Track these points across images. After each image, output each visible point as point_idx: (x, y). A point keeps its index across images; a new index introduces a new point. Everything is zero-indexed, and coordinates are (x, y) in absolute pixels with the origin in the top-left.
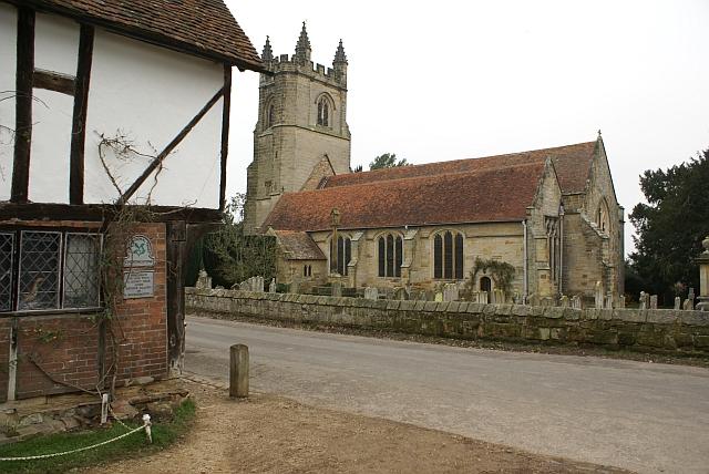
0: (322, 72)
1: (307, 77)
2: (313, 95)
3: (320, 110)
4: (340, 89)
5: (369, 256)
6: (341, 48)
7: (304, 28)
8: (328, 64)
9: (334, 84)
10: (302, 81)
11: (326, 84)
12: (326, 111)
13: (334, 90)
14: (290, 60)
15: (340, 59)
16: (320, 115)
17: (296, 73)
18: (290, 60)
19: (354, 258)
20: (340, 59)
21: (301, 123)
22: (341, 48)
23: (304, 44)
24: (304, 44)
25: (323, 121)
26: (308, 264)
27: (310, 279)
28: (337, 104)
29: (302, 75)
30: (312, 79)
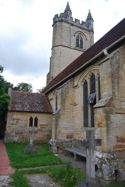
0: (78, 23)
1: (68, 23)
2: (73, 33)
3: (78, 40)
4: (89, 31)
5: (75, 105)
6: (90, 15)
7: (68, 4)
8: (83, 18)
9: (86, 28)
10: (64, 24)
11: (81, 28)
12: (82, 41)
13: (86, 31)
14: (59, 16)
15: (90, 18)
16: (77, 43)
17: (62, 21)
18: (59, 16)
19: (59, 107)
20: (90, 18)
21: (64, 44)
22: (90, 15)
23: (68, 10)
24: (68, 10)
25: (77, 45)
26: (34, 116)
27: (36, 129)
28: (88, 38)
29: (66, 22)
30: (72, 25)
